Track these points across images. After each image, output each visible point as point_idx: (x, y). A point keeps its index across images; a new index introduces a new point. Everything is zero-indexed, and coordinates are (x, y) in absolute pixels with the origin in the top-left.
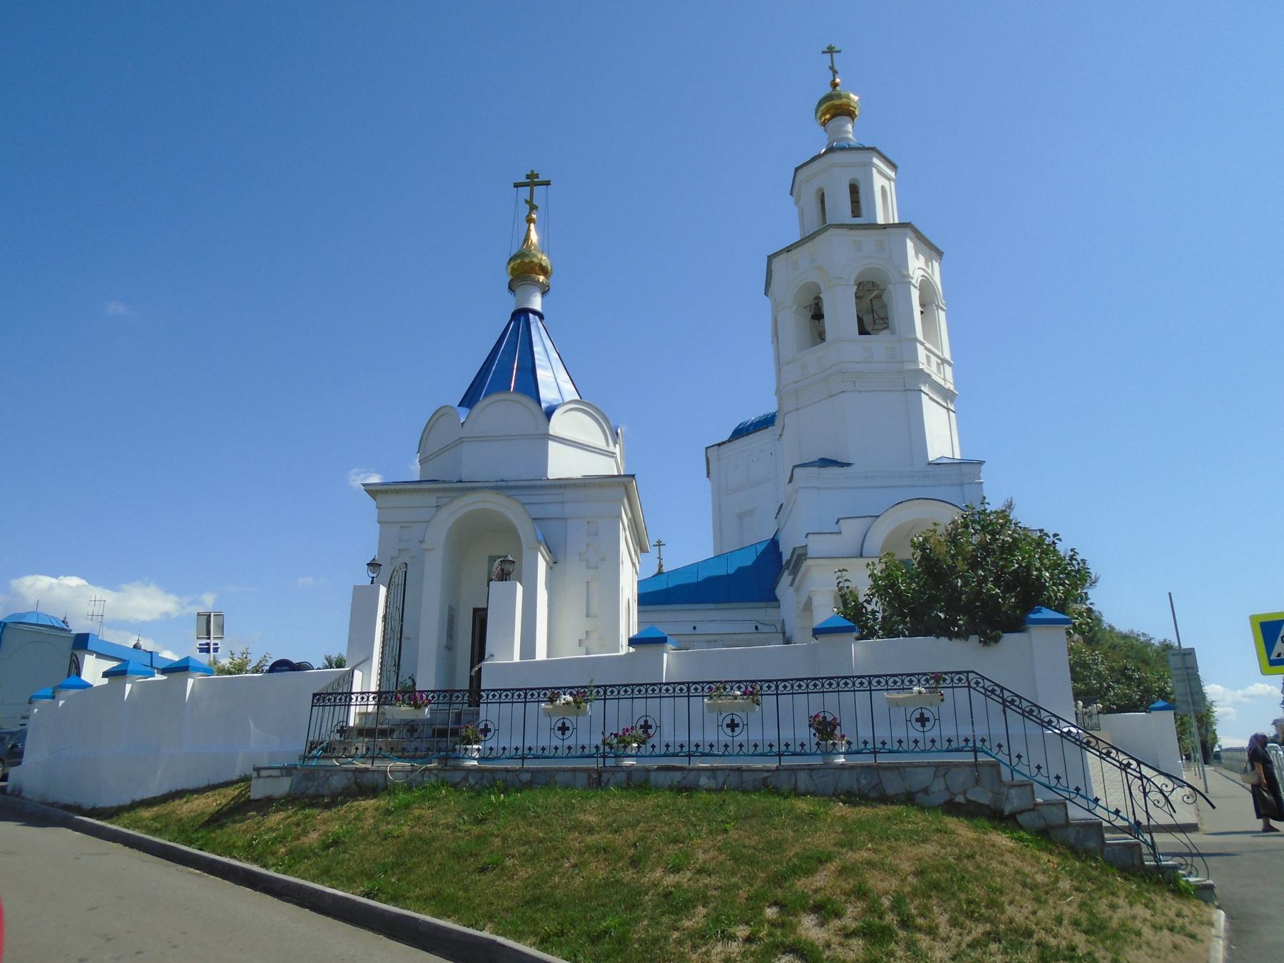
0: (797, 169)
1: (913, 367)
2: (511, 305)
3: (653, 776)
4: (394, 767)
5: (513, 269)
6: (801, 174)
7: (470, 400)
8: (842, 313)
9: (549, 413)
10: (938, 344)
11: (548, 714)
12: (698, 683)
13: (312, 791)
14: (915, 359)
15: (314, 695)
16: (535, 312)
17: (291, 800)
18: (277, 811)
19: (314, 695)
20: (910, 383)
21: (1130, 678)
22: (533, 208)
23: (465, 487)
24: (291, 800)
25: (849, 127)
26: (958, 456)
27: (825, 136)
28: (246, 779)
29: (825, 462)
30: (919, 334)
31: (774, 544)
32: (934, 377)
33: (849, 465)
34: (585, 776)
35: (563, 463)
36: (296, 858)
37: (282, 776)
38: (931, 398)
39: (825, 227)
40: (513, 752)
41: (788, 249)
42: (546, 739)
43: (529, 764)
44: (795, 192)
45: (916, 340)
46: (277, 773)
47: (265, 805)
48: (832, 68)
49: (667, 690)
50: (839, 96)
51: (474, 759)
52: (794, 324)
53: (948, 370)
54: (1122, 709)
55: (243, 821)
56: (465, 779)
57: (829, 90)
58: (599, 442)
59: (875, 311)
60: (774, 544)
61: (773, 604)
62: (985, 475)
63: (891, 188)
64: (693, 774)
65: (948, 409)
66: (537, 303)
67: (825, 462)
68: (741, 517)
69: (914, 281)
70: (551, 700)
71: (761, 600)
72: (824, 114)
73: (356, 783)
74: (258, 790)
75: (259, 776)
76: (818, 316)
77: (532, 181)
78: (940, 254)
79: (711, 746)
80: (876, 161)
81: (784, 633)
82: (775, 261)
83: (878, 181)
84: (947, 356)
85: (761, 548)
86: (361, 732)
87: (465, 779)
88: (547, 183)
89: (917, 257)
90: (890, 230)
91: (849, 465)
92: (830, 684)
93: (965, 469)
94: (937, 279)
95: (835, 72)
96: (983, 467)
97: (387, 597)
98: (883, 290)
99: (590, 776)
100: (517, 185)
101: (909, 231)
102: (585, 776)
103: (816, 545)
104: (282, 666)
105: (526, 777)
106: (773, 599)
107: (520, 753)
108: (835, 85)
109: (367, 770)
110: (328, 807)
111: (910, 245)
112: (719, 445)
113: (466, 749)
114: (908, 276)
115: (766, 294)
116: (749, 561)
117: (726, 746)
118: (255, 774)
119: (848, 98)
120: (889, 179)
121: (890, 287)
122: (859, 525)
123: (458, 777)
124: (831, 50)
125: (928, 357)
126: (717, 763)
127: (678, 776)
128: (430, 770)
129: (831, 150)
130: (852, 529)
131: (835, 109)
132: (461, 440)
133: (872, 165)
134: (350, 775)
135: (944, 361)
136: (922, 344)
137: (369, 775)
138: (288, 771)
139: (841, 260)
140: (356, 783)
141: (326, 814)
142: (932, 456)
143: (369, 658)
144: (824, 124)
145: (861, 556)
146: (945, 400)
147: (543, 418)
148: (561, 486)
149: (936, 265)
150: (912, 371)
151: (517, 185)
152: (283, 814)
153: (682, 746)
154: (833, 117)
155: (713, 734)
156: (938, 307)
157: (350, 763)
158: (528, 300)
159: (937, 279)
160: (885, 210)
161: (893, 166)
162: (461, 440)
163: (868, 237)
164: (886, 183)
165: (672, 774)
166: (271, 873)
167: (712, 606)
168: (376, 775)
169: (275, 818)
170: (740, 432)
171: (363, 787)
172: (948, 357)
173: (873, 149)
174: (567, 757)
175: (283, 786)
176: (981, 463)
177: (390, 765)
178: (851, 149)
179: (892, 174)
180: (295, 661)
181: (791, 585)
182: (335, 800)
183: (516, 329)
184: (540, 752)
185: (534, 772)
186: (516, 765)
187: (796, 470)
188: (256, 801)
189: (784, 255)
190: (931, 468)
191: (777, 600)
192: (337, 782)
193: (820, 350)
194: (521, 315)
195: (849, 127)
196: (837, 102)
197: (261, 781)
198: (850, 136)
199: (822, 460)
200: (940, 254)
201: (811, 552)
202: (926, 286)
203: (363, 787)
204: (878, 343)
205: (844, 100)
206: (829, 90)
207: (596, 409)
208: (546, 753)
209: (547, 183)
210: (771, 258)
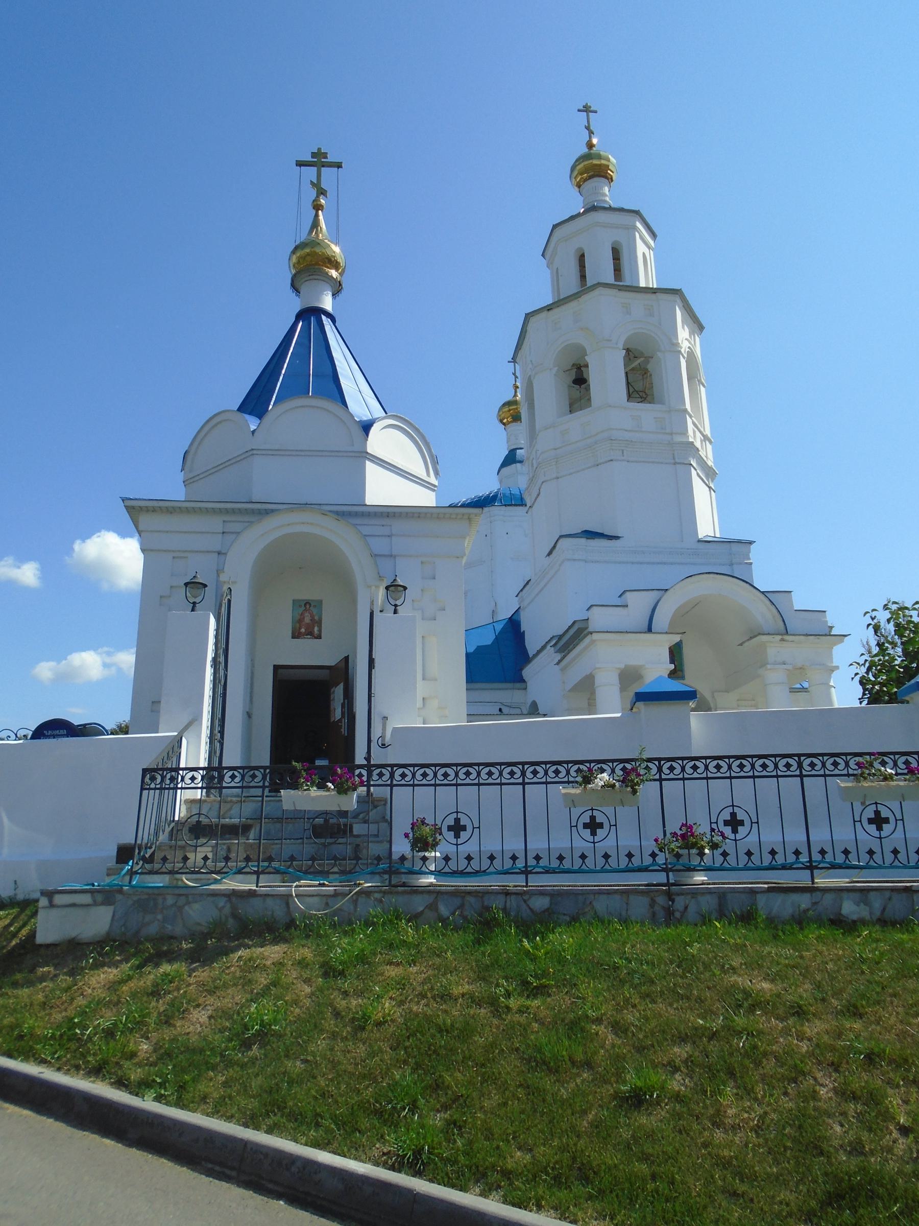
0: (555, 227)
2: (296, 305)
3: (761, 900)
4: (305, 891)
5: (299, 258)
6: (558, 233)
7: (255, 402)
8: (608, 377)
9: (366, 427)
11: (572, 802)
12: (559, 763)
13: (153, 929)
14: (685, 432)
15: (145, 771)
16: (328, 315)
17: (107, 948)
18: (97, 966)
19: (145, 771)
20: (680, 455)
22: (322, 192)
23: (261, 511)
24: (107, 948)
25: (606, 190)
27: (581, 199)
28: (25, 906)
29: (590, 534)
30: (688, 406)
34: (645, 900)
35: (381, 489)
36: (181, 1070)
37: (95, 904)
38: (698, 474)
40: (508, 864)
42: (564, 840)
43: (536, 881)
45: (686, 411)
46: (86, 899)
47: (71, 953)
48: (588, 128)
49: (490, 774)
50: (599, 157)
51: (431, 873)
55: (30, 983)
56: (433, 907)
57: (585, 150)
58: (418, 469)
59: (643, 379)
61: (518, 685)
62: (755, 555)
63: (651, 256)
64: (828, 898)
65: (710, 488)
66: (327, 303)
67: (590, 534)
69: (683, 351)
70: (587, 780)
71: (506, 681)
72: (581, 174)
73: (234, 915)
74: (49, 928)
75: (52, 905)
76: (580, 380)
77: (319, 160)
78: (701, 328)
79: (846, 852)
82: (533, 320)
83: (641, 248)
86: (198, 829)
87: (433, 907)
88: (339, 166)
89: (683, 328)
90: (660, 296)
92: (835, 764)
93: (735, 547)
95: (591, 133)
97: (217, 630)
98: (648, 359)
99: (653, 903)
100: (300, 164)
102: (645, 900)
103: (599, 619)
104: (53, 729)
105: (540, 903)
106: (519, 680)
107: (520, 864)
108: (590, 146)
109: (251, 894)
110: (200, 955)
113: (425, 859)
114: (677, 344)
117: (871, 853)
118: (44, 902)
119: (609, 160)
120: (649, 247)
121: (659, 354)
122: (651, 597)
123: (419, 904)
124: (587, 109)
125: (694, 432)
126: (861, 880)
127: (804, 901)
128: (366, 893)
129: (592, 209)
130: (639, 604)
131: (591, 169)
132: (251, 453)
133: (635, 228)
134: (222, 902)
135: (706, 438)
136: (691, 417)
137: (256, 902)
138: (107, 896)
140: (234, 915)
141: (203, 974)
142: (701, 535)
143: (196, 720)
144: (579, 186)
145: (650, 630)
146: (707, 476)
147: (361, 433)
148: (388, 515)
151: (300, 164)
152: (112, 973)
153: (797, 853)
154: (590, 177)
155: (841, 831)
156: (700, 382)
157: (216, 881)
158: (319, 299)
159: (698, 352)
160: (647, 277)
161: (654, 235)
162: (251, 453)
163: (638, 303)
164: (646, 251)
165: (795, 897)
166: (148, 1104)
168: (269, 901)
169: (98, 980)
171: (249, 925)
172: (708, 432)
173: (637, 213)
174: (603, 871)
175: (97, 922)
176: (751, 543)
177: (308, 885)
178: (610, 209)
179: (652, 242)
180: (77, 721)
181: (558, 663)
182: (206, 947)
183: (306, 330)
184: (555, 864)
185: (556, 895)
186: (515, 882)
188: (47, 946)
189: (544, 314)
190: (701, 545)
191: (524, 681)
192: (198, 914)
193: (582, 416)
194: (311, 314)
195: (606, 190)
196: (596, 162)
197: (54, 912)
198: (607, 199)
199: (586, 531)
203: (249, 925)
204: (645, 412)
205: (603, 162)
206: (585, 150)
207: (417, 430)
208: (567, 864)
209: (339, 166)
210: (528, 316)
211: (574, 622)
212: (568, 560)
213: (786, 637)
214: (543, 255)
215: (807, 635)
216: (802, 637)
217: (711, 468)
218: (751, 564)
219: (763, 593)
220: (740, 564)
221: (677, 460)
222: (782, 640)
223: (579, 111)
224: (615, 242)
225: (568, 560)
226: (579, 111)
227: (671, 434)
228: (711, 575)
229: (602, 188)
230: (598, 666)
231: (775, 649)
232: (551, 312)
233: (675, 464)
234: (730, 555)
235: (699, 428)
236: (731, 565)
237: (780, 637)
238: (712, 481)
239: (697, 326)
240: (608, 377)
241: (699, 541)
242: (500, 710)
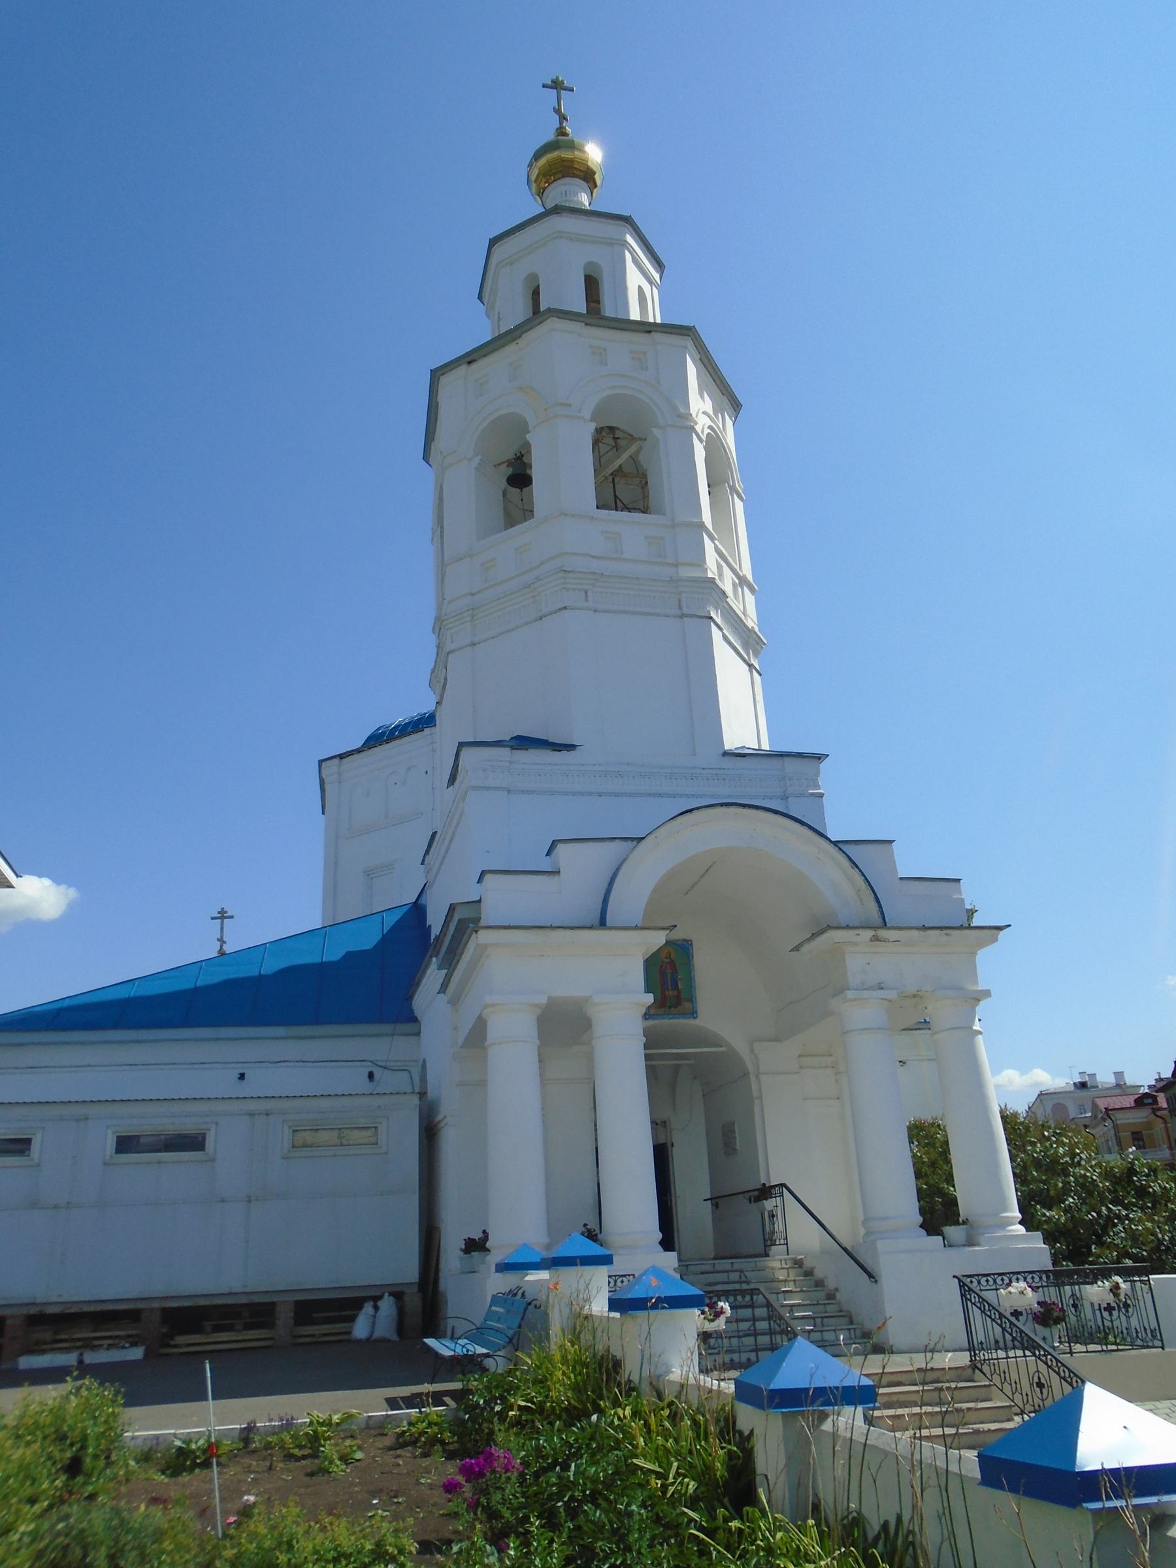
0: (493, 242)
1: (695, 573)
6: (500, 251)
8: (566, 469)
10: (735, 548)
14: (701, 562)
20: (691, 602)
21: (1142, 1192)
26: (766, 746)
29: (522, 742)
30: (707, 517)
31: (418, 910)
32: (731, 600)
33: (571, 747)
38: (725, 638)
39: (537, 313)
41: (470, 358)
44: (485, 300)
45: (702, 525)
48: (557, 111)
52: (470, 488)
53: (750, 599)
57: (550, 136)
59: (628, 473)
60: (418, 910)
65: (750, 666)
67: (522, 742)
68: (369, 874)
69: (698, 428)
71: (381, 1019)
76: (520, 478)
81: (422, 1094)
82: (444, 381)
83: (634, 279)
84: (747, 571)
85: (391, 920)
90: (657, 336)
91: (571, 747)
93: (791, 765)
94: (730, 440)
96: (824, 766)
101: (689, 343)
103: (502, 899)
108: (561, 132)
111: (692, 370)
112: (341, 757)
115: (426, 458)
116: (368, 940)
120: (651, 281)
121: (656, 432)
124: (556, 85)
125: (719, 567)
130: (582, 866)
131: (558, 165)
133: (625, 244)
135: (743, 581)
136: (712, 538)
139: (566, 379)
142: (730, 743)
145: (602, 923)
146: (746, 646)
149: (729, 423)
150: (695, 580)
156: (733, 489)
159: (730, 440)
161: (659, 265)
163: (618, 345)
167: (280, 1031)
170: (377, 739)
172: (747, 571)
173: (627, 220)
176: (820, 757)
179: (657, 276)
181: (443, 988)
187: (466, 753)
189: (463, 370)
190: (729, 762)
191: (413, 1019)
200: (735, 406)
201: (489, 915)
202: (714, 444)
210: (436, 375)
211: (452, 908)
212: (475, 788)
213: (883, 933)
214: (480, 298)
215: (925, 928)
216: (915, 933)
217: (752, 631)
218: (821, 796)
219: (836, 843)
220: (802, 795)
221: (685, 611)
222: (876, 939)
223: (544, 86)
224: (590, 265)
225: (475, 788)
226: (544, 86)
227: (676, 566)
228: (732, 810)
229: (576, 194)
230: (489, 999)
231: (863, 959)
232: (474, 366)
233: (682, 616)
234: (781, 781)
235: (729, 556)
236: (785, 798)
237: (869, 933)
238: (756, 655)
239: (729, 399)
240: (566, 469)
241: (726, 754)
242: (371, 1076)
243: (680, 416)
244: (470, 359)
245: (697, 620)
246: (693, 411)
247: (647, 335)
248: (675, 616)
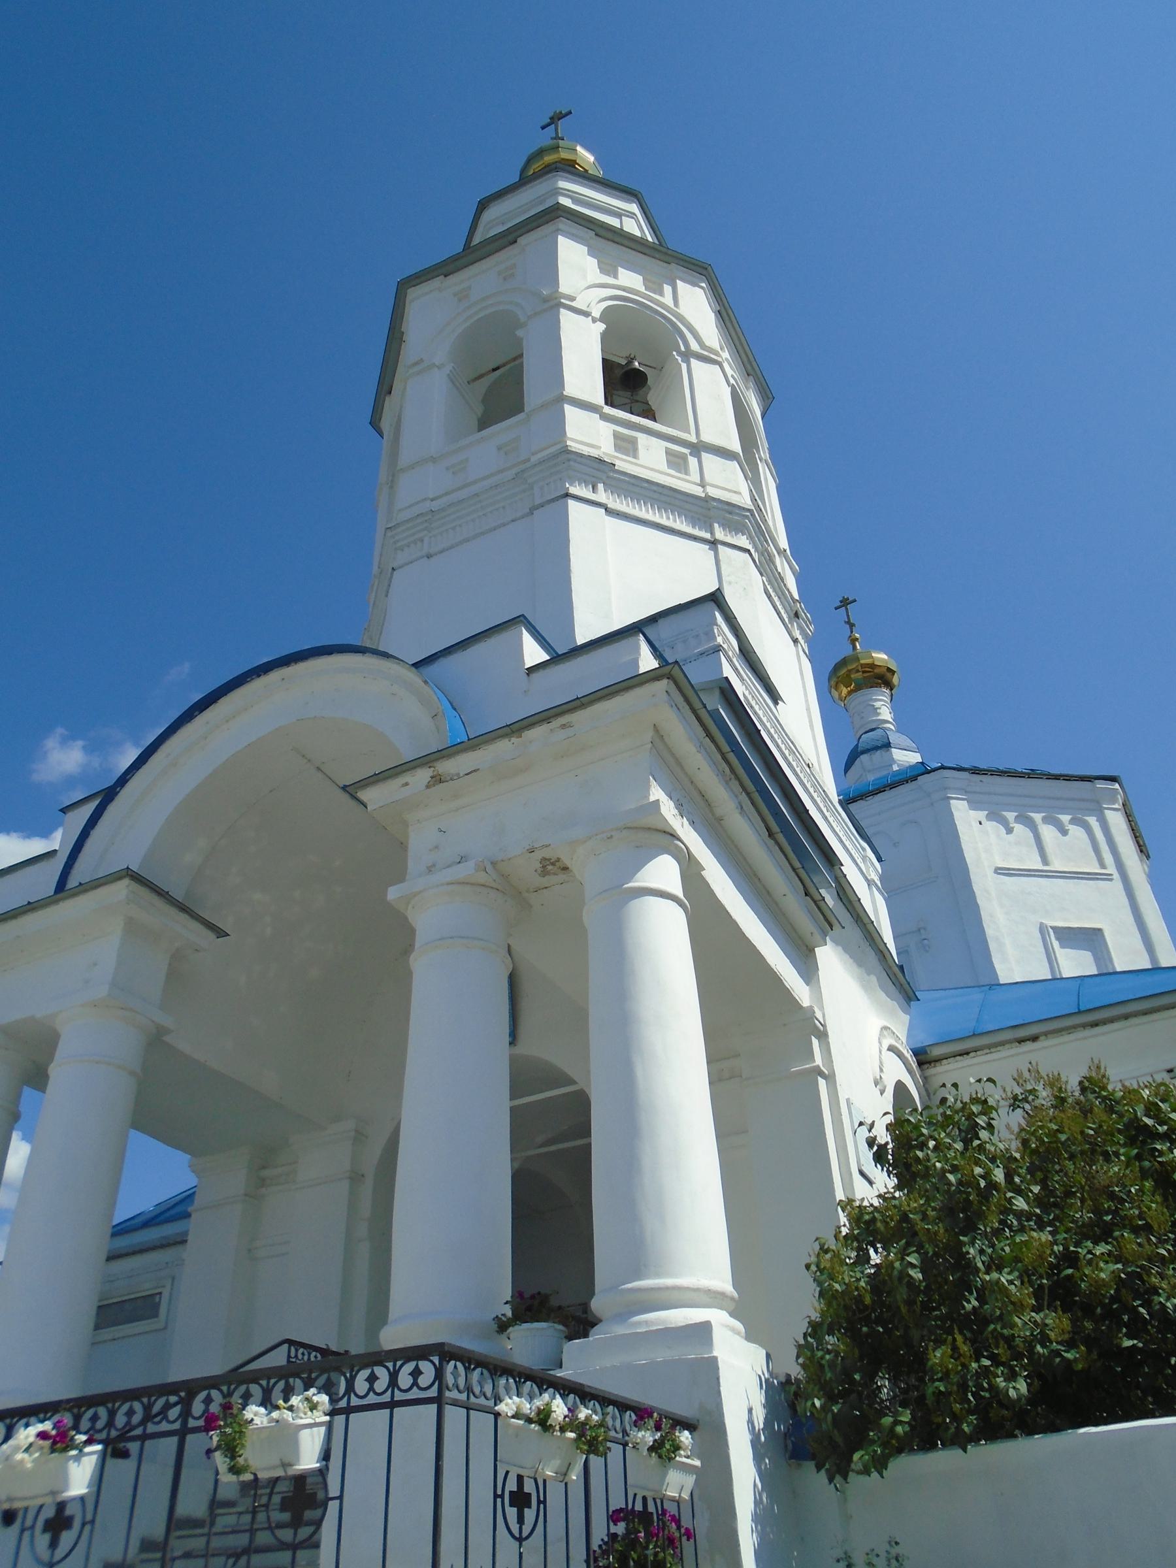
38: (609, 511)
54: (1067, 1400)
65: (713, 544)
80: (563, 184)
101: (562, 223)
121: (520, 333)
156: (688, 355)
179: (634, 208)
213: (447, 767)
216: (504, 746)
222: (438, 779)
223: (543, 128)
237: (422, 776)
243: (546, 300)
244: (386, 388)
245: (553, 505)
246: (565, 287)
247: (515, 245)
248: (527, 515)
